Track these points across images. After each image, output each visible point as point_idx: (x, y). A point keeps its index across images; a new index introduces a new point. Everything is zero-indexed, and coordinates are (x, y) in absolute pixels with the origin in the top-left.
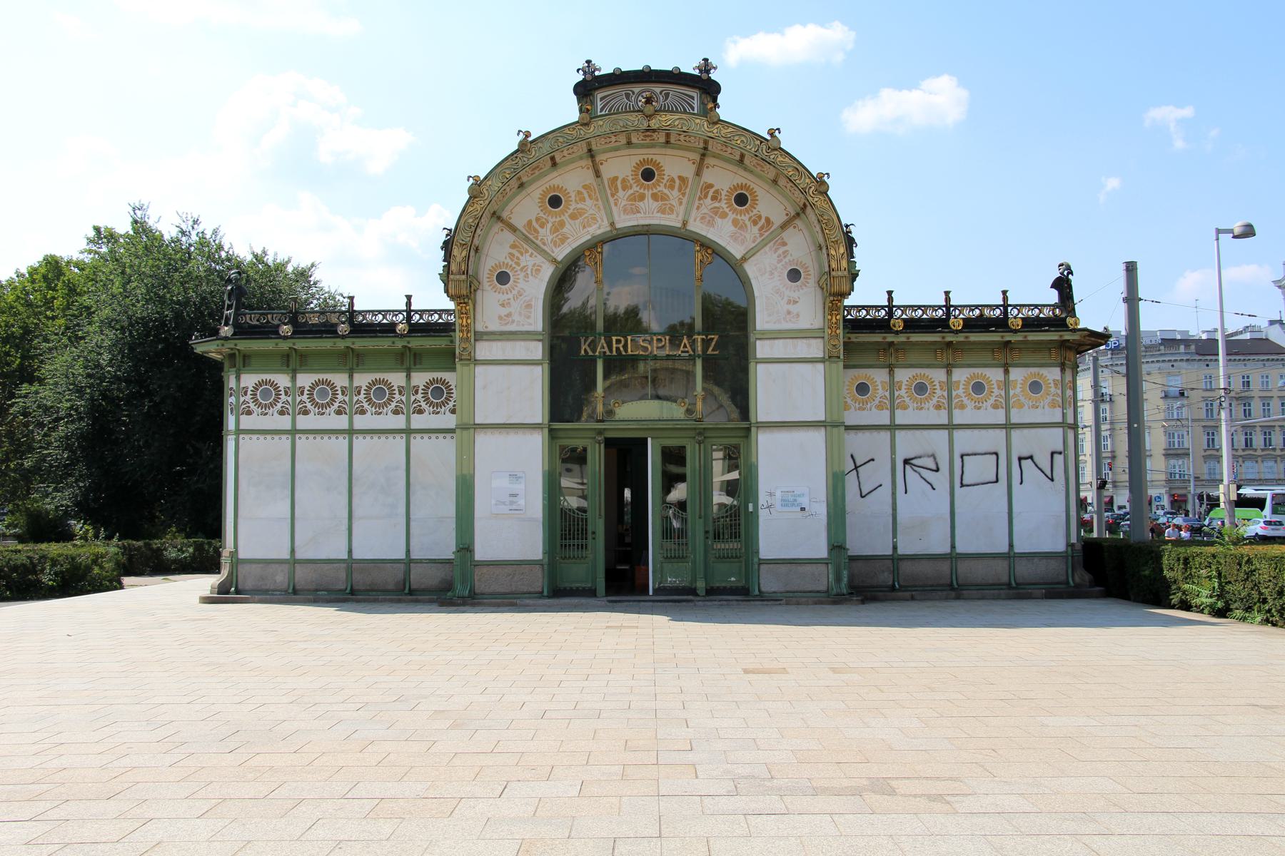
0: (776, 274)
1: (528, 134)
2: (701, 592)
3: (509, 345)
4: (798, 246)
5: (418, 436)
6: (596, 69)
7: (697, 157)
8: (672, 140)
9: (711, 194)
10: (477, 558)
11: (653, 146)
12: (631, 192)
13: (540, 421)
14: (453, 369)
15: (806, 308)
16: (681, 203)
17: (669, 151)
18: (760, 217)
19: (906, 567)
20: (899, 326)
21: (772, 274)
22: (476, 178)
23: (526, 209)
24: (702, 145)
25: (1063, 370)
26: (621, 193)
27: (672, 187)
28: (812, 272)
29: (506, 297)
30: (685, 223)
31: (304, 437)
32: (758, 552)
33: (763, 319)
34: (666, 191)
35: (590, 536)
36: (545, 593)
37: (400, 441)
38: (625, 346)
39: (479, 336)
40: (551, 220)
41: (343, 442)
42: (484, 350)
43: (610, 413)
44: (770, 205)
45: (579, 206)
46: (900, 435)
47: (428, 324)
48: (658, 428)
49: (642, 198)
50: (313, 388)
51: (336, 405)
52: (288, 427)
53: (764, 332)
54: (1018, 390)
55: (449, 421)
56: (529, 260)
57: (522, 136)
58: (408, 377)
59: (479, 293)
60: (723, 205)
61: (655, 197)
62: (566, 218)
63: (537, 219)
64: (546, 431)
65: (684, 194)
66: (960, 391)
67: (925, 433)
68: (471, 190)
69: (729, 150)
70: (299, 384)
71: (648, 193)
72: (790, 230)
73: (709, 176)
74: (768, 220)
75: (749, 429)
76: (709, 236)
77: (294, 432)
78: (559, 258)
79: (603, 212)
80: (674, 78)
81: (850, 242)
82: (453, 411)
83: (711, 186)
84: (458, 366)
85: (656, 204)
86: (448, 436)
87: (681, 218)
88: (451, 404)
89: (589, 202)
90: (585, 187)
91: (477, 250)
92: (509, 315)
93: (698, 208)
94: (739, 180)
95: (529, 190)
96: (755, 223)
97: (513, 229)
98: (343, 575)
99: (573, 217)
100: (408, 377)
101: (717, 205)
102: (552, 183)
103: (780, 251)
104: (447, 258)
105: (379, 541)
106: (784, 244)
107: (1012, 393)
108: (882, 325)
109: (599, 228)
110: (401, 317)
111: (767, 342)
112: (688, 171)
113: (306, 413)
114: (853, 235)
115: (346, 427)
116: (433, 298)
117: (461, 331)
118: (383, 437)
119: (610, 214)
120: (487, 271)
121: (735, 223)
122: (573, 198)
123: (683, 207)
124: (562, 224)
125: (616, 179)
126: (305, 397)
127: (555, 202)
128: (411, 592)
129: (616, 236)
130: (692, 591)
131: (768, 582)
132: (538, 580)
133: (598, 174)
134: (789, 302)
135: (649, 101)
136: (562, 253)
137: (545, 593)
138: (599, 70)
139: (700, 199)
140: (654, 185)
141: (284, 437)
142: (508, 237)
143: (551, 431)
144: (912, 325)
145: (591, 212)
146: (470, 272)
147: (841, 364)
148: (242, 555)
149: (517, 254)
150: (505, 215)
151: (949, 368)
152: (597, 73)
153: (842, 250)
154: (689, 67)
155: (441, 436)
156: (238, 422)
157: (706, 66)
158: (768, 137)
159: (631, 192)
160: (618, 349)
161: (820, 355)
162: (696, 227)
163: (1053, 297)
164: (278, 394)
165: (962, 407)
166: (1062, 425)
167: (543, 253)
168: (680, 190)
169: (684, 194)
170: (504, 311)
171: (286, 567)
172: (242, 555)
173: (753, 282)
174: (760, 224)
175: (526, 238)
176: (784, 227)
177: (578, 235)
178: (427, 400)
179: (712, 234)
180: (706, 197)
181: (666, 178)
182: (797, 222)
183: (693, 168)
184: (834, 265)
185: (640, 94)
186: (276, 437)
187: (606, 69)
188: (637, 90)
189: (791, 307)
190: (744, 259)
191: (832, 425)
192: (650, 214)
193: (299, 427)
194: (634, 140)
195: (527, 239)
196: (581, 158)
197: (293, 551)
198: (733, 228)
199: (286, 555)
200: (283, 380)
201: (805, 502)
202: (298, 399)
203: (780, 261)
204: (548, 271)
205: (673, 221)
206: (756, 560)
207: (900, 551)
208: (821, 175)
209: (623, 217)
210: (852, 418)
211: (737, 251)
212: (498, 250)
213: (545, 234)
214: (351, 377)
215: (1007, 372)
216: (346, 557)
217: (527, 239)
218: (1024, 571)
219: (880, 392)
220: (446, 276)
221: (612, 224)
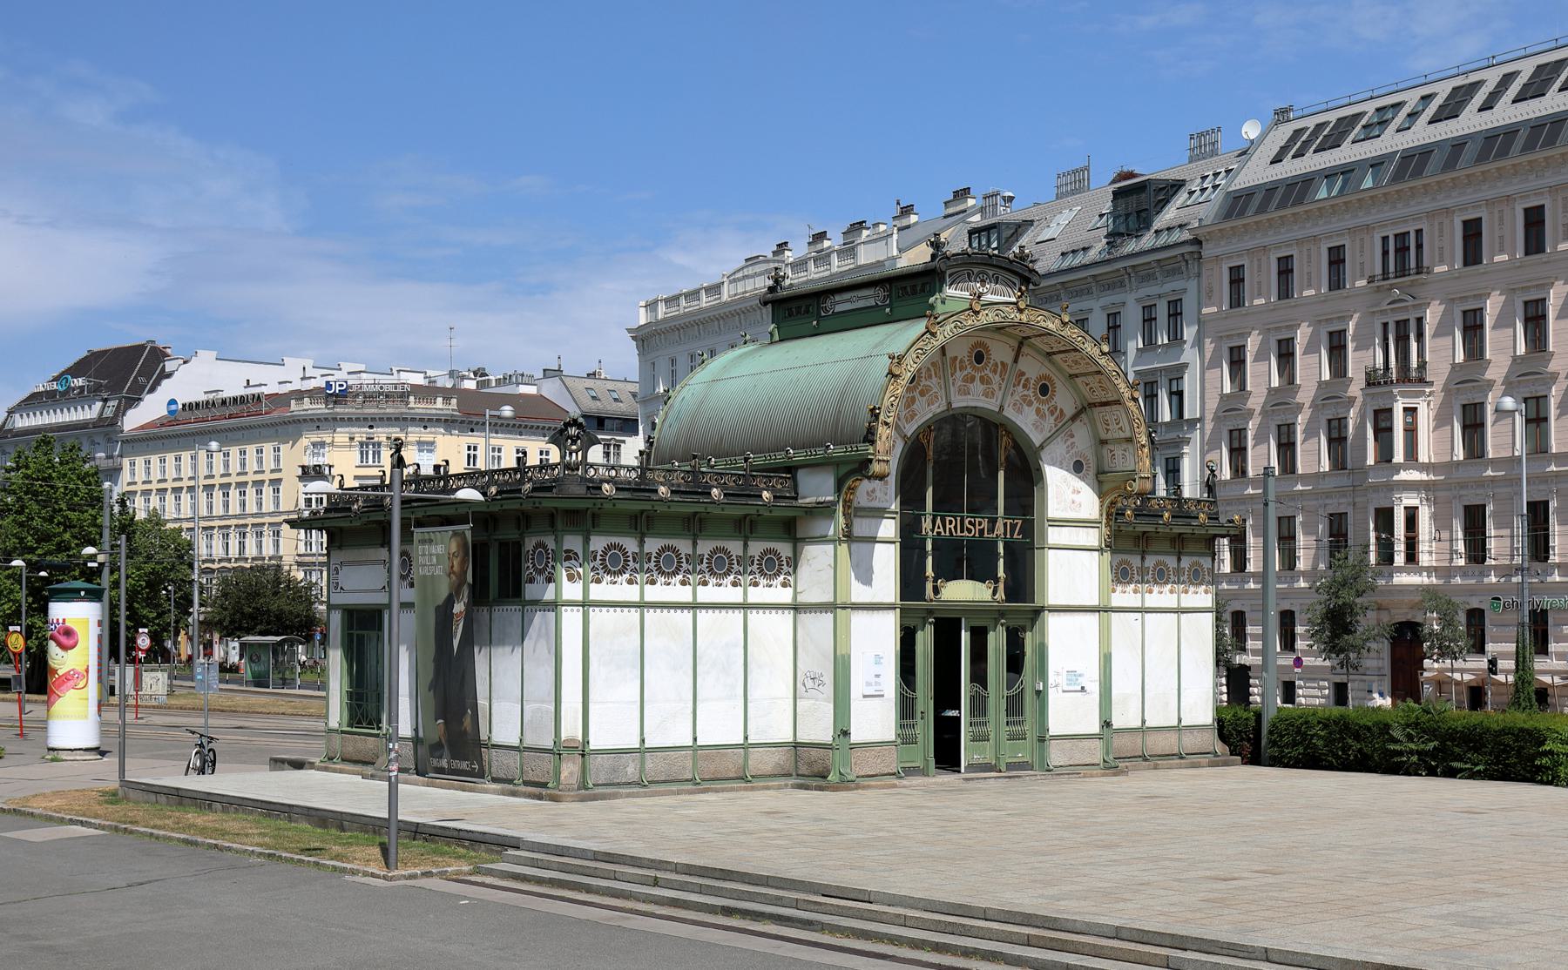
2: (1003, 768)
4: (1082, 436)
13: (892, 600)
17: (997, 336)
27: (995, 372)
33: (1054, 510)
35: (919, 715)
41: (687, 615)
43: (936, 591)
48: (972, 609)
49: (973, 379)
52: (637, 598)
58: (746, 546)
61: (982, 380)
71: (978, 376)
73: (1024, 364)
82: (784, 585)
83: (1023, 374)
89: (934, 380)
94: (1045, 371)
96: (1052, 413)
98: (689, 764)
99: (922, 394)
100: (746, 546)
105: (719, 728)
106: (1072, 436)
109: (938, 408)
112: (1009, 360)
119: (947, 396)
121: (1038, 411)
140: (983, 369)
156: (586, 591)
161: (1096, 544)
162: (1009, 413)
176: (1074, 418)
183: (1013, 354)
188: (976, 271)
189: (1075, 497)
190: (1042, 447)
201: (1083, 682)
211: (1037, 439)
214: (695, 544)
215: (1179, 560)
218: (1191, 742)
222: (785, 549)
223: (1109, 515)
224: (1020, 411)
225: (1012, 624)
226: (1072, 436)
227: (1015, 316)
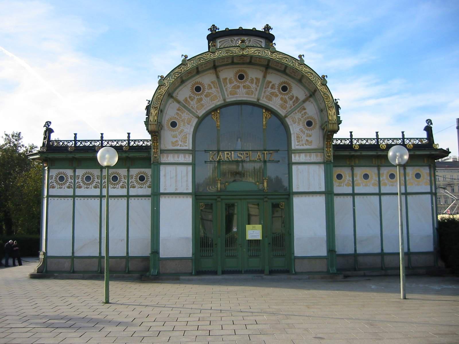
0: (301, 123)
1: (186, 57)
3: (176, 155)
4: (311, 110)
5: (133, 198)
6: (217, 29)
7: (264, 69)
8: (253, 61)
9: (271, 85)
10: (161, 256)
11: (243, 64)
12: (233, 85)
14: (149, 167)
15: (315, 139)
16: (256, 90)
18: (293, 97)
19: (361, 259)
20: (357, 148)
21: (299, 123)
22: (162, 77)
23: (184, 93)
24: (266, 63)
25: (430, 168)
26: (229, 85)
27: (252, 83)
28: (318, 122)
29: (175, 133)
30: (258, 100)
31: (79, 199)
32: (294, 254)
33: (294, 145)
34: (250, 85)
36: (193, 273)
37: (124, 201)
38: (231, 156)
39: (163, 151)
40: (196, 97)
42: (165, 158)
44: (298, 92)
45: (210, 91)
46: (357, 198)
47: (138, 146)
49: (238, 87)
50: (83, 176)
51: (95, 184)
52: (72, 194)
53: (294, 150)
54: (410, 177)
55: (148, 191)
56: (186, 115)
57: (183, 57)
58: (128, 171)
59: (162, 132)
60: (276, 91)
62: (203, 96)
63: (190, 97)
64: (194, 196)
65: (258, 86)
66: (384, 177)
67: (368, 197)
68: (160, 82)
69: (280, 65)
70: (77, 174)
72: (308, 101)
73: (269, 78)
74: (297, 98)
75: (289, 195)
76: (270, 105)
77: (74, 196)
78: (200, 115)
79: (220, 94)
80: (253, 33)
81: (338, 107)
82: (149, 187)
83: (270, 82)
84: (152, 166)
85: (245, 91)
86: (147, 198)
87: (256, 97)
88: (148, 183)
89: (214, 89)
90: (212, 82)
91: (161, 111)
92: (177, 141)
93: (265, 92)
95: (186, 84)
97: (179, 102)
99: (206, 96)
100: (128, 171)
101: (273, 91)
102: (197, 80)
103: (303, 112)
104: (148, 114)
106: (305, 109)
107: (407, 178)
108: (350, 147)
109: (219, 102)
110: (125, 143)
111: (297, 155)
113: (80, 187)
114: (339, 104)
115: (99, 194)
116: (141, 135)
117: (154, 149)
118: (116, 199)
119: (223, 95)
120: (166, 121)
122: (206, 87)
123: (257, 92)
124: (201, 99)
125: (226, 79)
126: (80, 180)
127: (198, 89)
128: (129, 272)
129: (227, 105)
130: (262, 272)
131: (298, 267)
132: (190, 267)
133: (218, 77)
134: (307, 136)
135: (243, 41)
136: (201, 113)
137: (193, 273)
138: (218, 29)
139: (265, 88)
140: (245, 82)
141: (70, 199)
142: (176, 105)
143: (196, 196)
144: (362, 147)
145: (215, 94)
146: (159, 121)
147: (332, 165)
148: (49, 254)
149: (180, 113)
150: (174, 95)
151: (379, 167)
152: (217, 31)
153: (334, 111)
154: (260, 28)
155: (143, 198)
157: (268, 28)
158: (299, 59)
159: (233, 85)
160: (227, 157)
162: (264, 101)
163: (424, 135)
164: (67, 179)
165: (385, 185)
166: (430, 193)
167: (192, 112)
168: (256, 84)
169: (258, 86)
170: (175, 139)
171: (69, 260)
172: (49, 254)
173: (291, 127)
174: (293, 100)
175: (184, 106)
176: (304, 101)
177: (209, 104)
178: (137, 181)
179: (270, 105)
180: (268, 87)
181: (250, 78)
182: (311, 99)
184: (330, 118)
185: (237, 40)
186: (66, 199)
187: (222, 28)
188: (236, 38)
189: (308, 138)
190: (286, 116)
191: (329, 194)
192: (242, 95)
193: (76, 194)
194: (235, 61)
195: (185, 107)
196: (210, 69)
197: (73, 253)
198: (281, 102)
199: (70, 254)
200: (69, 172)
202: (77, 181)
203: (302, 117)
204: (195, 121)
205: (252, 98)
206: (293, 257)
207: (358, 252)
208: (323, 77)
209: (230, 96)
210: (337, 190)
211: (282, 112)
212: (171, 111)
213: (193, 104)
216: (98, 255)
217: (185, 107)
219: (348, 178)
220: (147, 123)
221: (224, 100)
222: (148, 171)
223: (327, 144)
224: (270, 99)
225: (275, 201)
226: (305, 109)
227: (236, 51)
